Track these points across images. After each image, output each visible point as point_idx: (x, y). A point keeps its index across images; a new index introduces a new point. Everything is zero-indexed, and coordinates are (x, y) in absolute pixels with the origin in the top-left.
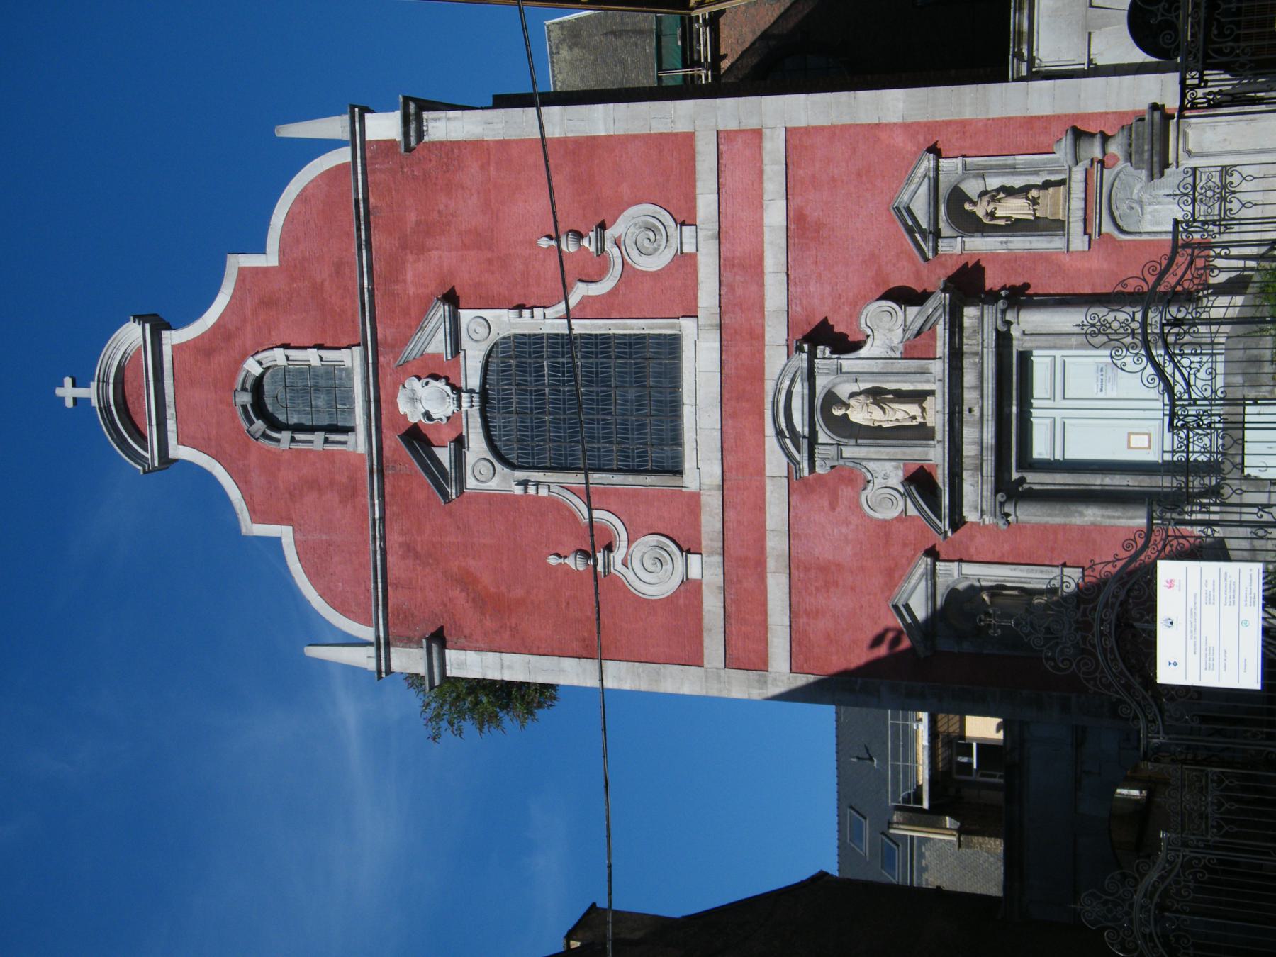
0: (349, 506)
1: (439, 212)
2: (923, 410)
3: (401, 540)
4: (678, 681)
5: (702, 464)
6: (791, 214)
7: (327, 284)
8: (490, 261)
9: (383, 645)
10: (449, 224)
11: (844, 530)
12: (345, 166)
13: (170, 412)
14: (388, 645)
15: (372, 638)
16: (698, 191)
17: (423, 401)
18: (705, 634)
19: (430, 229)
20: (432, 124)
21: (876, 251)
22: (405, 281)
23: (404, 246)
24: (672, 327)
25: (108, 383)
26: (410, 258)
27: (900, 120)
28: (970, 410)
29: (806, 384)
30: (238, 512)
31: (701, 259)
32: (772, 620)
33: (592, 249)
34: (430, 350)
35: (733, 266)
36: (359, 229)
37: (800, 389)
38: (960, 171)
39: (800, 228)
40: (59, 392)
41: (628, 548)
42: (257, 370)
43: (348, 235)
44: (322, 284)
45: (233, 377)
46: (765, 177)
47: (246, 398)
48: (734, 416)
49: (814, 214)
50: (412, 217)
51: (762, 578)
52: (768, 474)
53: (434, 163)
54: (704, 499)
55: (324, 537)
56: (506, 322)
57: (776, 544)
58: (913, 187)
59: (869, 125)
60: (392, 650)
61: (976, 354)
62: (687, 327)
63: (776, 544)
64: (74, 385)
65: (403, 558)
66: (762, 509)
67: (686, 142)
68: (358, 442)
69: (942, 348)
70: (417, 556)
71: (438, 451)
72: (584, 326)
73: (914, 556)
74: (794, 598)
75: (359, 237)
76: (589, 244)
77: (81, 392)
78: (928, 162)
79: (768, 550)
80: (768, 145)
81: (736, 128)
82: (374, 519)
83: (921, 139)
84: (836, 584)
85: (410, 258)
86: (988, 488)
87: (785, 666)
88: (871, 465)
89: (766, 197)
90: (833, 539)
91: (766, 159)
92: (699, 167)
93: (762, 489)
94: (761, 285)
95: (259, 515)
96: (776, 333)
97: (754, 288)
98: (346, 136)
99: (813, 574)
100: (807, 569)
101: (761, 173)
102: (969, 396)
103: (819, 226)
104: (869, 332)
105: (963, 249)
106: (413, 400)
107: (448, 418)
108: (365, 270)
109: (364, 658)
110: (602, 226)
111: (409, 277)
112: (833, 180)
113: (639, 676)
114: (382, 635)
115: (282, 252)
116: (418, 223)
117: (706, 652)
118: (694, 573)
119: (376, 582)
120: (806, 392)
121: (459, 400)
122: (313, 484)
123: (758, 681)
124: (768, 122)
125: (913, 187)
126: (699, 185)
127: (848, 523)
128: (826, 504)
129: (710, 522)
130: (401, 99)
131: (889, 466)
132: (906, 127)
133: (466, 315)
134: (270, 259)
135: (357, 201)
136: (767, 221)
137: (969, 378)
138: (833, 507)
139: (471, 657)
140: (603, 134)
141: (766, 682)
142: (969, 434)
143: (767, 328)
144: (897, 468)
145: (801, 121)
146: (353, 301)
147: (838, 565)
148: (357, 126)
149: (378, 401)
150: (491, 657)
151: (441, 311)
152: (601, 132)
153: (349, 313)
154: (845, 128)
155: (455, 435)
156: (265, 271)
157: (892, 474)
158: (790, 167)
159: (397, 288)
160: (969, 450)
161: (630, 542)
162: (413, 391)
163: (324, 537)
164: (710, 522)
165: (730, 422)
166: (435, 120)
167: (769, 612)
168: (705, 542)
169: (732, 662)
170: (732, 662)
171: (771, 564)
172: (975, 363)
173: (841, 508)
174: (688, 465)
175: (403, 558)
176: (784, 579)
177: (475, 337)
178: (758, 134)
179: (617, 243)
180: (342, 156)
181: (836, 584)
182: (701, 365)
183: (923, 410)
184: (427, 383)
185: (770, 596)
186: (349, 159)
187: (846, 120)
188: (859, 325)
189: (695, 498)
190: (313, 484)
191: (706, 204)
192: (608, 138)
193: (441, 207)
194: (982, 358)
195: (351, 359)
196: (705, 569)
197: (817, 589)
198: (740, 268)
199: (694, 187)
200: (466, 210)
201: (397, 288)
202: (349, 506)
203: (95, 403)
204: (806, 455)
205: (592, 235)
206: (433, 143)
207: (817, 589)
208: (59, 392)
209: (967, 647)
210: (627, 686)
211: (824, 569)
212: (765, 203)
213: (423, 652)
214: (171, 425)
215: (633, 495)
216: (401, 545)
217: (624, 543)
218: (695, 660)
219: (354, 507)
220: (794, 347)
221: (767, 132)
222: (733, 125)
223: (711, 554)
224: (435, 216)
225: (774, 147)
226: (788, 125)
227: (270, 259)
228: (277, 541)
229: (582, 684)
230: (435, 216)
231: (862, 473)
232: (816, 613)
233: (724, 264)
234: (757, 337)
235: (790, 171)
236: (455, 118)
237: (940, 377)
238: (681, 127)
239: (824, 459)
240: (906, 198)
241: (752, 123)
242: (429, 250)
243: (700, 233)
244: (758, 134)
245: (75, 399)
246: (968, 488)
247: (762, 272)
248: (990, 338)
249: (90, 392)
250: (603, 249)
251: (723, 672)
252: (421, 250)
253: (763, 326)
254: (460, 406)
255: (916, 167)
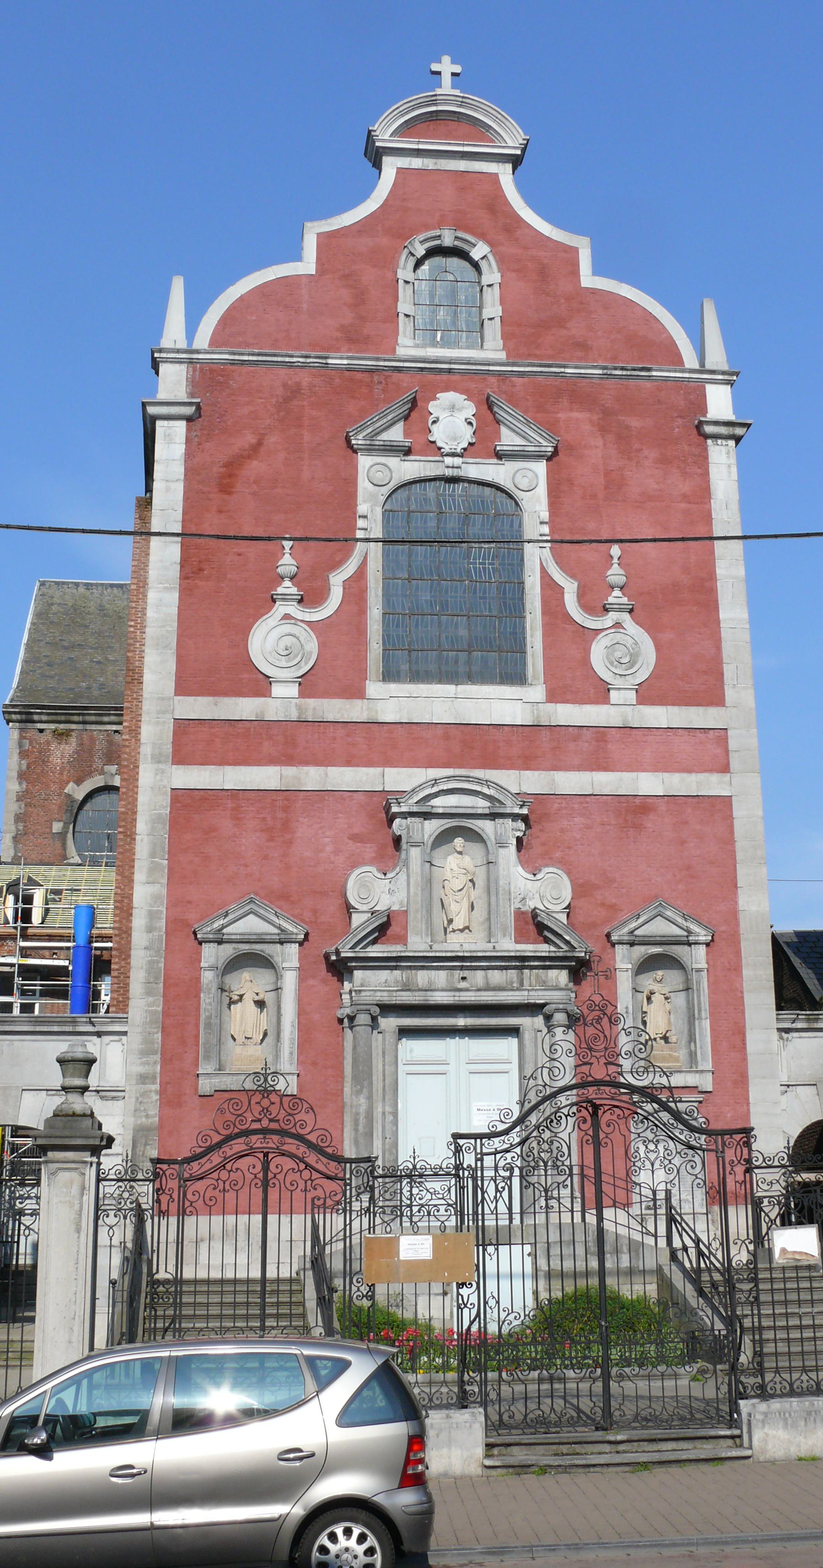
0: (339, 334)
1: (641, 450)
2: (462, 931)
3: (304, 384)
4: (158, 669)
5: (393, 701)
6: (649, 800)
7: (563, 332)
8: (594, 496)
9: (188, 357)
10: (630, 459)
11: (329, 849)
12: (681, 363)
13: (429, 163)
14: (190, 362)
15: (196, 346)
16: (669, 707)
17: (451, 419)
18: (211, 698)
19: (623, 440)
20: (723, 449)
21: (615, 885)
22: (571, 410)
23: (607, 413)
24: (534, 677)
25: (460, 106)
26: (595, 418)
27: (741, 909)
28: (464, 978)
29: (487, 811)
30: (329, 221)
31: (604, 708)
32: (229, 770)
33: (611, 600)
34: (503, 430)
35: (598, 741)
36: (622, 369)
37: (482, 805)
38: (695, 966)
39: (636, 809)
40: (446, 59)
41: (302, 621)
42: (476, 254)
43: (614, 359)
44: (566, 328)
45: (467, 230)
46: (685, 775)
47: (448, 240)
48: (447, 737)
49: (650, 822)
50: (635, 423)
51: (271, 761)
52: (387, 770)
53: (686, 448)
54: (359, 702)
55: (305, 306)
56: (536, 507)
57: (311, 777)
58: (680, 920)
59: (736, 877)
60: (184, 367)
61: (522, 984)
62: (537, 692)
63: (311, 777)
64: (453, 74)
65: (285, 385)
66: (349, 762)
67: (716, 699)
68: (408, 346)
69: (528, 949)
70: (287, 400)
71: (400, 426)
72: (533, 587)
73: (303, 921)
74: (253, 794)
75: (615, 369)
76: (616, 597)
77: (447, 79)
78: (703, 935)
79: (306, 769)
80: (714, 778)
81: (730, 748)
82: (326, 358)
83: (723, 928)
84: (271, 839)
85: (595, 418)
86: (385, 998)
87: (178, 784)
88: (403, 877)
89: (666, 775)
90: (315, 838)
91: (702, 777)
92: (692, 709)
93: (370, 764)
94: (579, 768)
95: (326, 241)
96: (533, 782)
97: (576, 762)
98: (709, 366)
99: (280, 815)
100: (286, 809)
101: (689, 771)
102: (478, 977)
103: (638, 827)
104: (539, 876)
105: (621, 970)
106: (453, 408)
107: (434, 442)
108: (583, 371)
109: (173, 334)
110: (631, 611)
111: (576, 415)
112: (683, 843)
113: (163, 626)
114: (201, 356)
115: (594, 292)
116: (628, 428)
117: (191, 699)
118: (277, 690)
119: (259, 355)
120: (480, 811)
121: (453, 455)
122: (360, 299)
123: (161, 754)
124: (736, 779)
125: (680, 920)
126: (675, 709)
127: (337, 852)
128: (356, 830)
129: (334, 709)
130: (749, 422)
131: (402, 895)
132: (733, 916)
133: (541, 468)
134: (588, 279)
135: (649, 370)
136: (643, 776)
137: (496, 977)
138: (355, 838)
139: (178, 449)
140: (722, 616)
141: (159, 762)
142: (440, 977)
143: (536, 773)
144: (401, 903)
145: (738, 812)
146: (550, 357)
147: (290, 843)
148: (720, 377)
149: (449, 371)
150: (179, 470)
151: (545, 444)
152: (723, 615)
153: (538, 352)
154: (732, 854)
155: (415, 447)
156: (575, 272)
157: (394, 899)
158: (695, 800)
159: (565, 402)
160: (422, 977)
161: (309, 623)
162: (460, 410)
163: (305, 306)
164: (334, 709)
165: (440, 731)
166: (728, 453)
167: (238, 768)
168: (311, 702)
169: (183, 727)
170: (183, 727)
171: (290, 771)
172: (512, 983)
173: (352, 846)
174: (394, 688)
175: (285, 385)
176: (274, 785)
177: (519, 475)
178: (725, 768)
179: (618, 625)
180: (690, 360)
181: (271, 839)
182: (496, 704)
183: (462, 931)
184: (470, 423)
185: (255, 769)
186: (687, 366)
187: (739, 856)
188: (547, 865)
189: (360, 694)
190: (360, 299)
191: (659, 716)
192: (718, 622)
193: (646, 452)
194: (518, 989)
195: (493, 350)
196: (283, 701)
197: (264, 819)
198: (597, 748)
199: (674, 704)
200: (644, 477)
201: (565, 402)
202: (339, 334)
203: (439, 91)
204: (415, 809)
205: (625, 600)
206: (705, 449)
207: (264, 819)
208: (446, 59)
209: (208, 977)
210: (150, 613)
211: (286, 826)
212: (660, 774)
213: (183, 396)
214: (417, 163)
215: (361, 630)
216: (298, 384)
217: (308, 617)
218: (183, 687)
219: (337, 339)
220: (522, 798)
221: (726, 777)
222: (732, 744)
223: (299, 708)
224: (636, 446)
225: (711, 785)
226: (734, 798)
227: (588, 279)
228: (298, 257)
229: (151, 565)
230: (636, 446)
231: (394, 869)
232: (237, 818)
233: (601, 733)
234: (527, 762)
235: (690, 800)
236: (730, 473)
237: (498, 948)
238: (730, 694)
239: (408, 827)
240: (669, 913)
241: (734, 764)
242: (603, 436)
243: (628, 709)
244: (725, 768)
245: (439, 73)
246: (384, 975)
247: (593, 770)
248: (538, 997)
249: (446, 87)
250: (613, 610)
251: (169, 716)
252: (603, 430)
253: (537, 769)
254: (448, 455)
255: (700, 924)
